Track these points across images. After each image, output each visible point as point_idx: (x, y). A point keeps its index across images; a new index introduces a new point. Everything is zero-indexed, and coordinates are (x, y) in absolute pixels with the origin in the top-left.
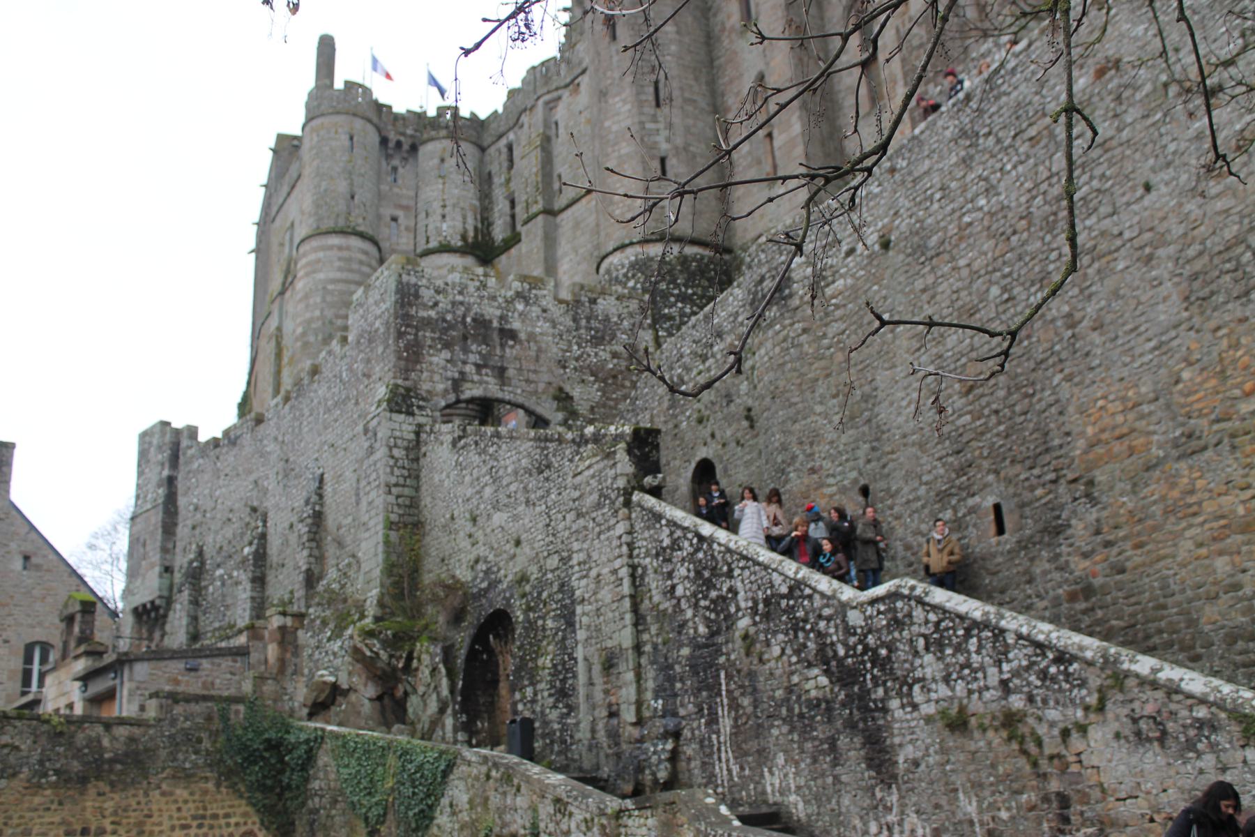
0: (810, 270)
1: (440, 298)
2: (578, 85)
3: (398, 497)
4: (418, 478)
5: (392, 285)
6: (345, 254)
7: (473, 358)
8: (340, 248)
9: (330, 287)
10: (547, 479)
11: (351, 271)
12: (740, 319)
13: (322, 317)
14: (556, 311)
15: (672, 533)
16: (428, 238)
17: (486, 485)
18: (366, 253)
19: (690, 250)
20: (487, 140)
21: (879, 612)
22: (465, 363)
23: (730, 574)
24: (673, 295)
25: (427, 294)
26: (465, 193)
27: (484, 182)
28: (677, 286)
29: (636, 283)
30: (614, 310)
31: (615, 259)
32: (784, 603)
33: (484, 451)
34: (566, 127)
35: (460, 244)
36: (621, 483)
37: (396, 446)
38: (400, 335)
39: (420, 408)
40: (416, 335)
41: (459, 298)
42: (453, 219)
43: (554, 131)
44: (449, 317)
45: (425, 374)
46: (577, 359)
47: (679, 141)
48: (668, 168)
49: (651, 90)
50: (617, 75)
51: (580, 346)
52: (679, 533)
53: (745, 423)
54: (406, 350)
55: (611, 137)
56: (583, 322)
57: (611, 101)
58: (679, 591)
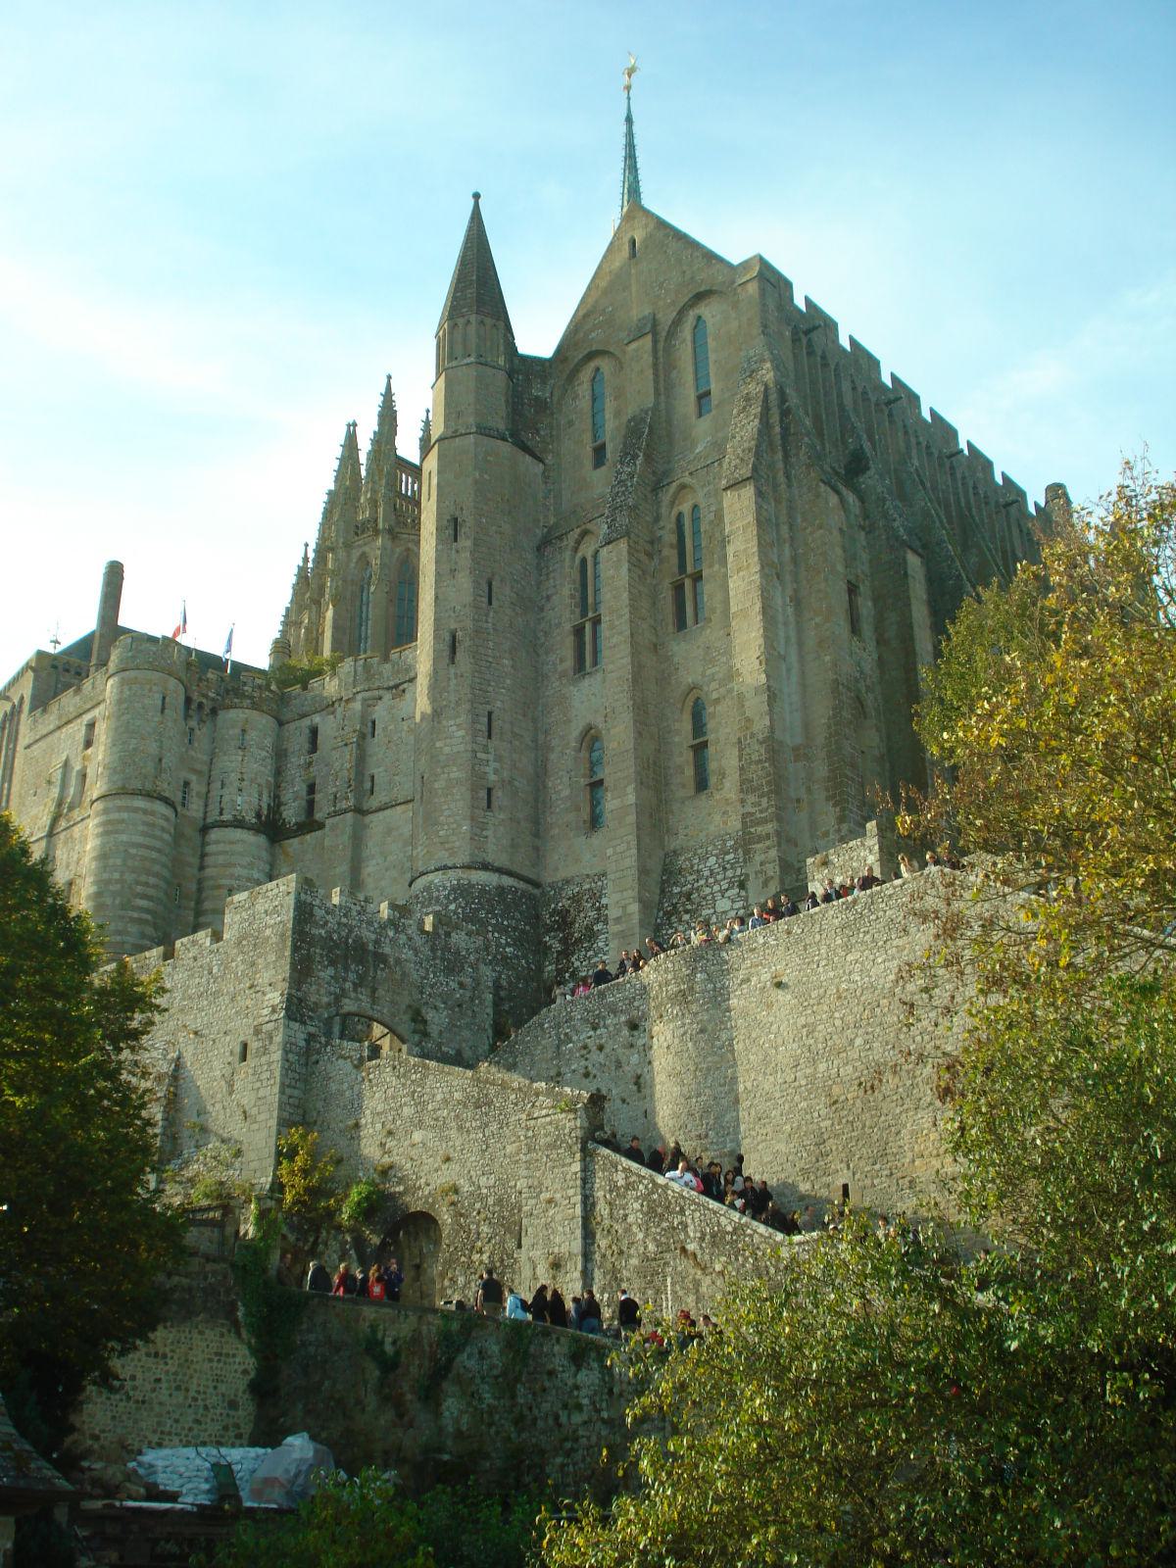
0: (710, 986)
1: (329, 917)
2: (404, 691)
3: (290, 1097)
4: (306, 1081)
5: (291, 901)
6: (150, 819)
7: (352, 976)
8: (145, 812)
9: (133, 851)
10: (486, 1114)
11: (153, 837)
12: (636, 1004)
13: (121, 881)
14: (419, 941)
15: (627, 1178)
16: (222, 810)
17: (405, 1104)
18: (167, 819)
19: (507, 881)
20: (287, 715)
21: (804, 1250)
22: (345, 980)
23: (682, 1211)
24: (490, 924)
25: (319, 913)
26: (263, 769)
27: (280, 755)
28: (495, 916)
29: (457, 908)
30: (463, 944)
31: (436, 878)
32: (728, 1237)
33: (404, 1075)
34: (385, 729)
35: (254, 820)
36: (579, 1133)
37: (291, 1051)
38: (295, 949)
39: (311, 1018)
40: (309, 950)
41: (344, 920)
42: (250, 795)
43: (370, 730)
44: (335, 937)
45: (314, 987)
46: (432, 987)
47: (505, 774)
48: (493, 798)
49: (486, 719)
50: (453, 698)
51: (435, 973)
52: (633, 1178)
53: (635, 1088)
54: (301, 962)
55: (442, 758)
56: (439, 953)
57: (444, 723)
58: (631, 1219)
